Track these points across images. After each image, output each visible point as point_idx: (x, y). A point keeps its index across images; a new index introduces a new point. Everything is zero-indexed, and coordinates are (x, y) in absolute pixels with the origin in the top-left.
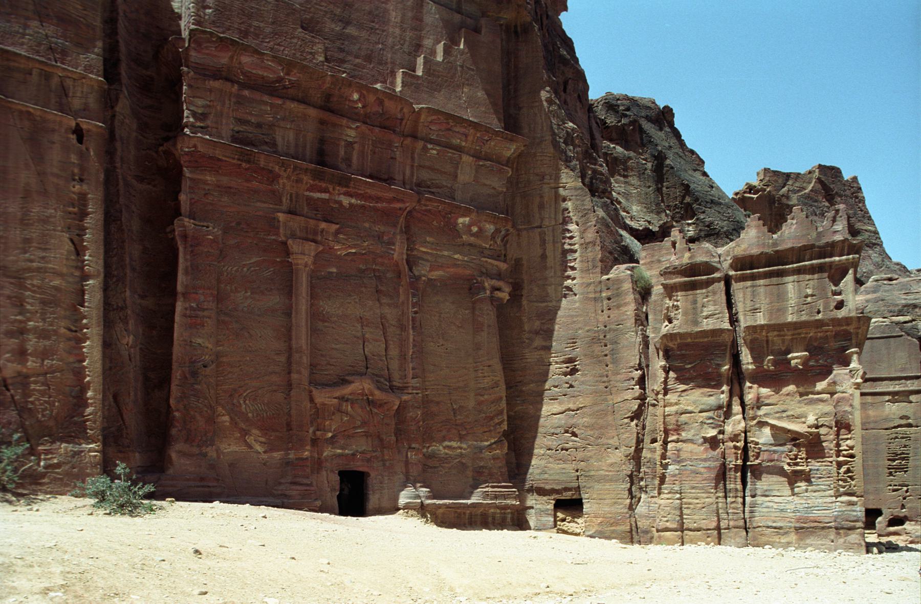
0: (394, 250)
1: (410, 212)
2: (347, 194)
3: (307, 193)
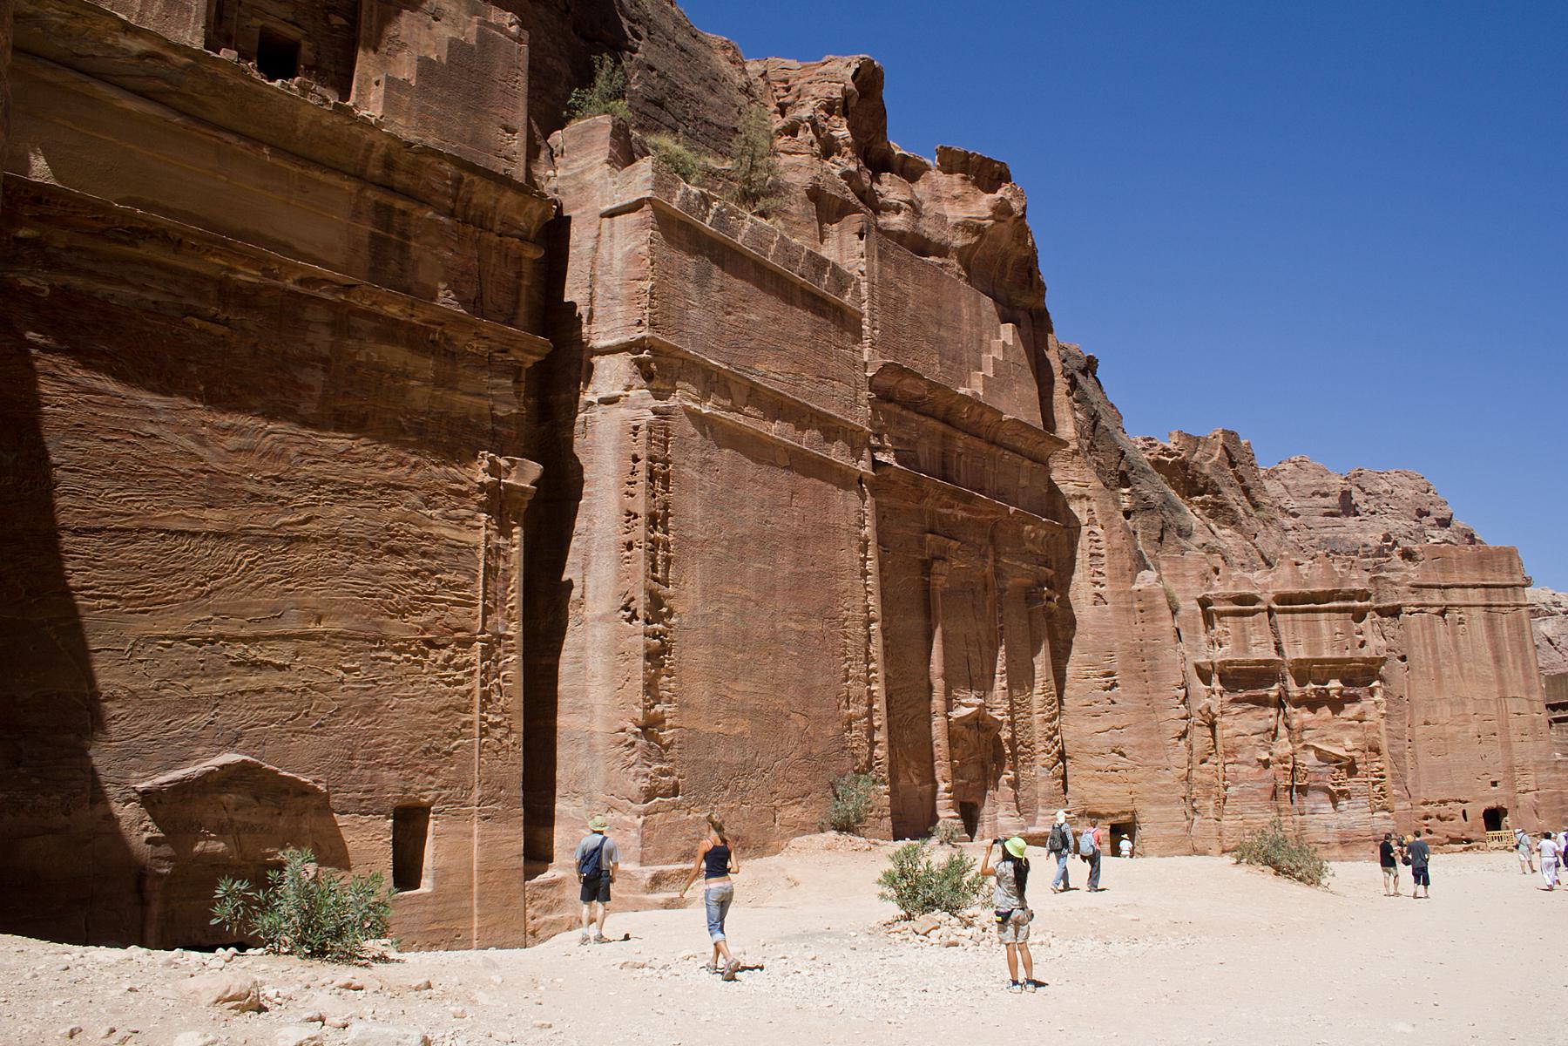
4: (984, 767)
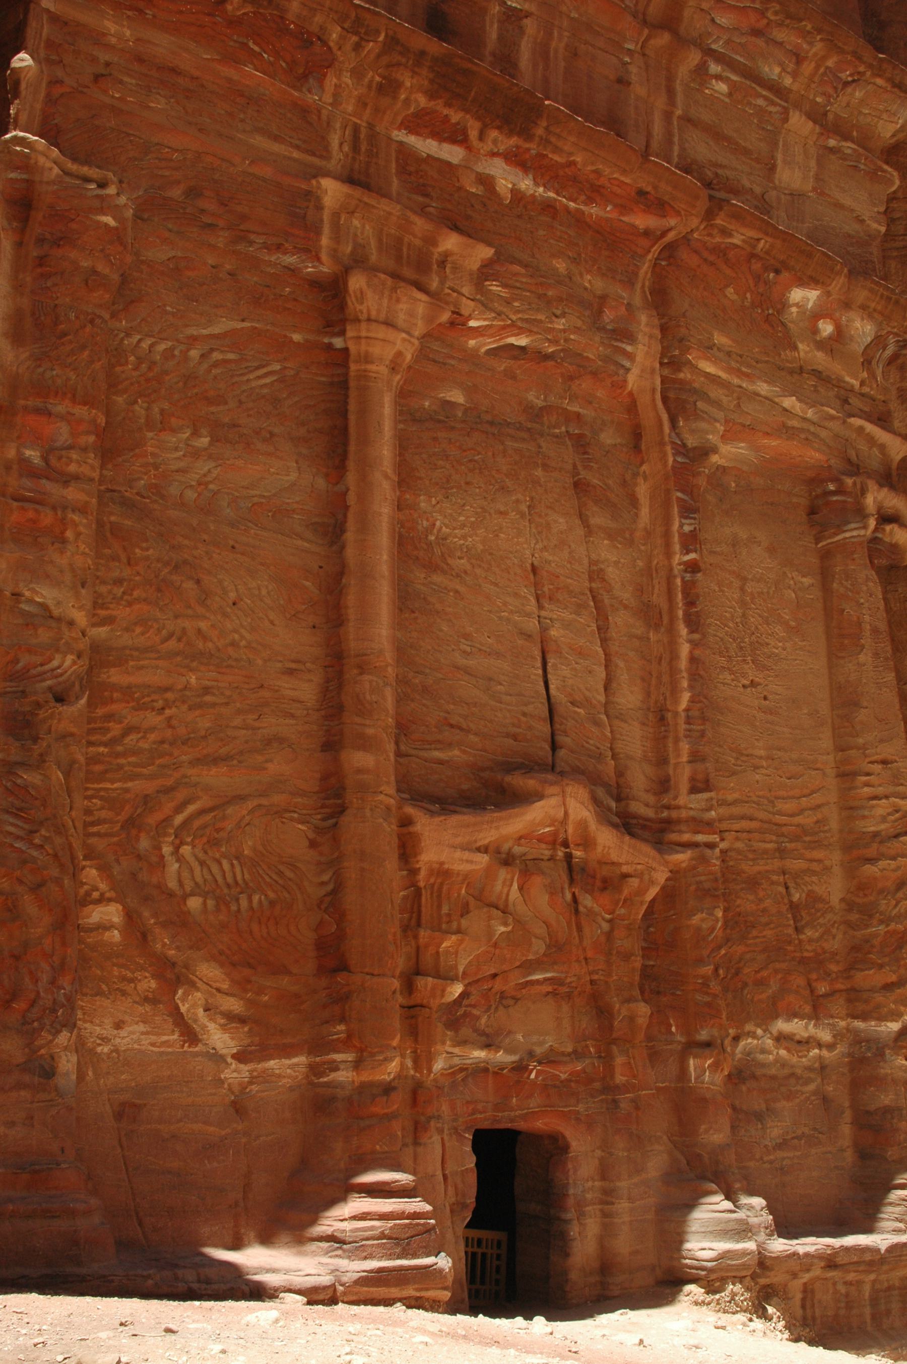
1: (671, 247)
2: (515, 159)
3: (400, 135)
4: (602, 1012)
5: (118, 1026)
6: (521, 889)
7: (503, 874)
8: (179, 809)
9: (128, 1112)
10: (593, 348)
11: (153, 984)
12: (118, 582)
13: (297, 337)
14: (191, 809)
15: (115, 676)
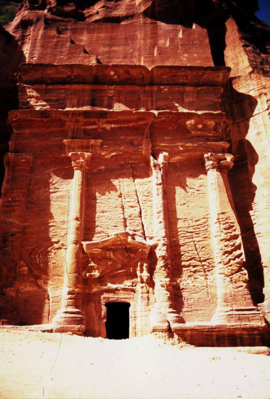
0: (142, 149)
3: (83, 127)
5: (26, 287)
6: (114, 255)
7: (108, 253)
8: (40, 249)
9: (26, 301)
10: (131, 149)
11: (33, 279)
12: (29, 215)
13: (67, 167)
14: (42, 249)
15: (28, 230)
